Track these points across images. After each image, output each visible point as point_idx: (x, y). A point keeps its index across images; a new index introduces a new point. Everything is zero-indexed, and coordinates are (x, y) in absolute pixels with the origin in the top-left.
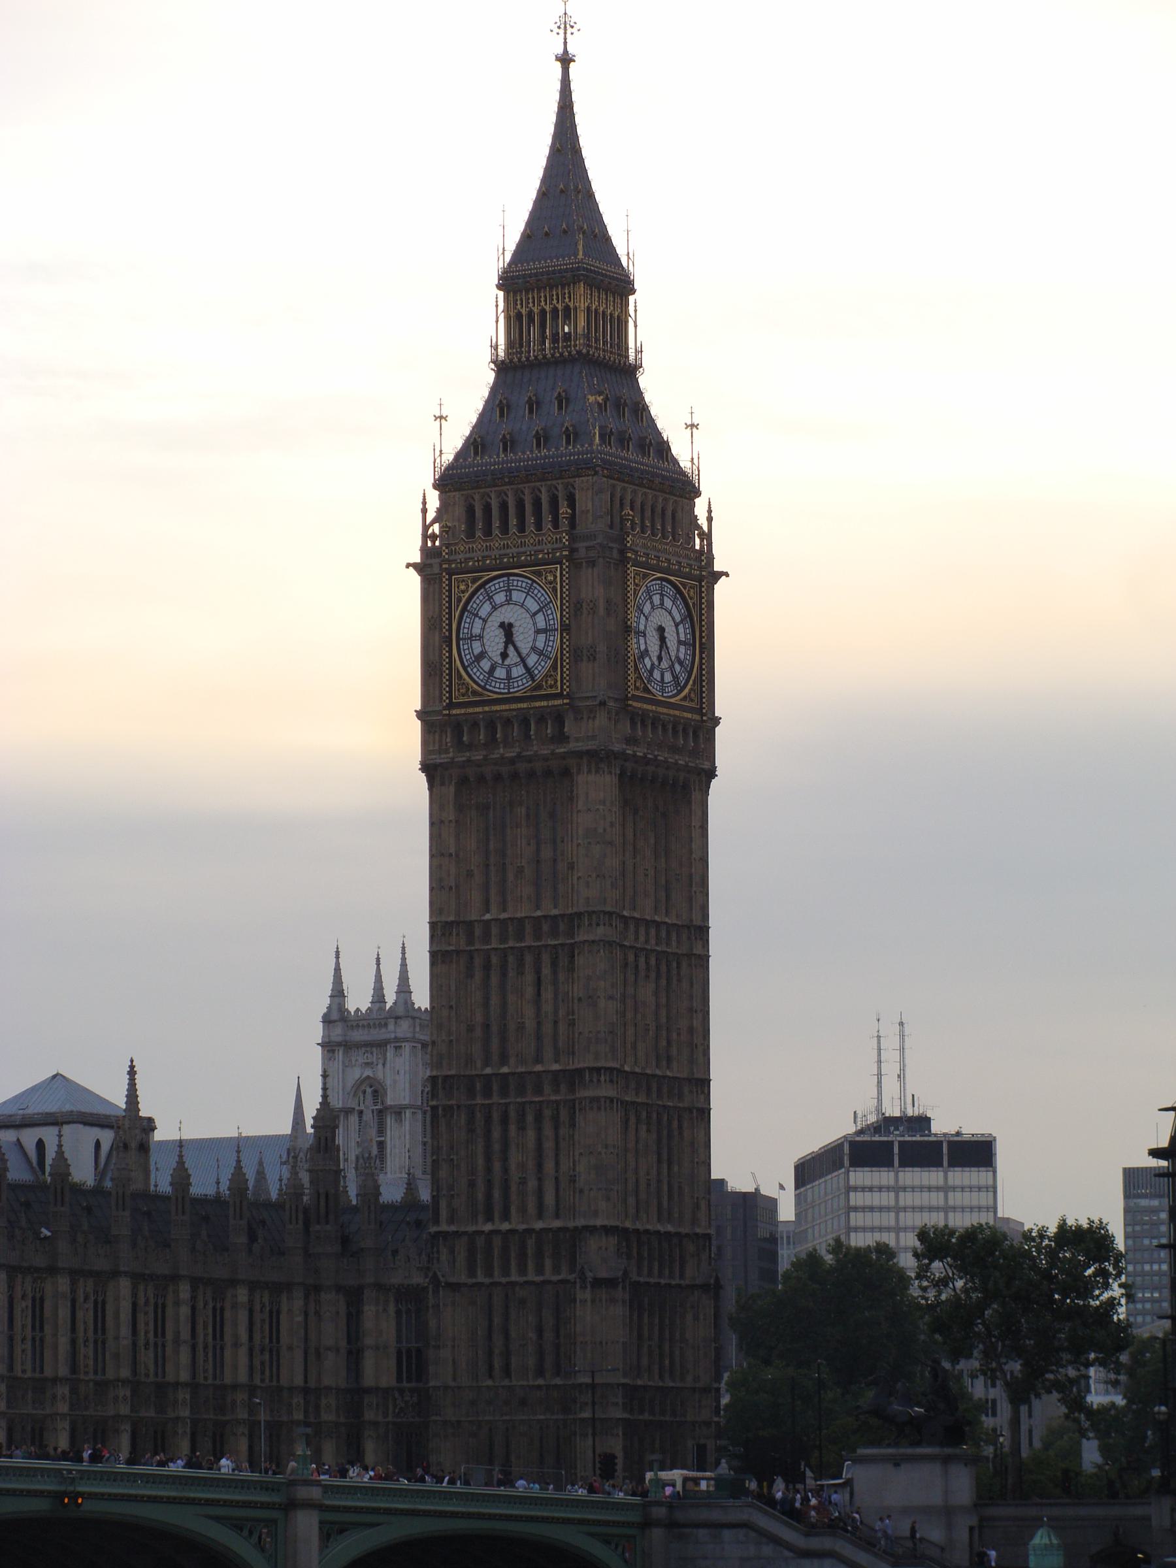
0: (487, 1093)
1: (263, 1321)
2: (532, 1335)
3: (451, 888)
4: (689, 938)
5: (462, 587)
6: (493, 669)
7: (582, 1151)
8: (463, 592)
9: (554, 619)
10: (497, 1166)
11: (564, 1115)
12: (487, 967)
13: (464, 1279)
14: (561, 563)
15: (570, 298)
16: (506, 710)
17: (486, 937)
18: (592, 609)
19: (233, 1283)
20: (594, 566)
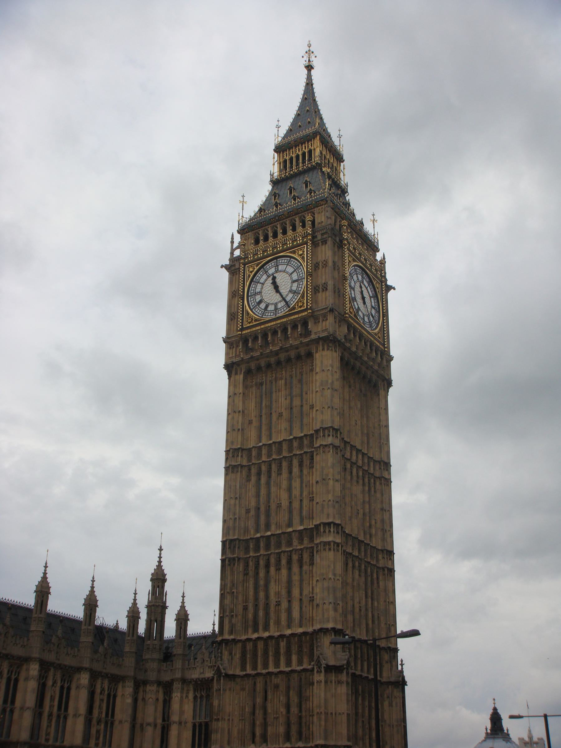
0: (257, 549)
1: (102, 700)
2: (283, 710)
3: (239, 430)
4: (380, 468)
5: (251, 269)
6: (267, 306)
7: (318, 578)
8: (251, 272)
9: (302, 273)
10: (262, 594)
11: (306, 557)
12: (259, 474)
13: (238, 672)
14: (306, 243)
15: (312, 146)
16: (274, 325)
17: (259, 455)
18: (324, 265)
19: (79, 670)
20: (326, 243)
